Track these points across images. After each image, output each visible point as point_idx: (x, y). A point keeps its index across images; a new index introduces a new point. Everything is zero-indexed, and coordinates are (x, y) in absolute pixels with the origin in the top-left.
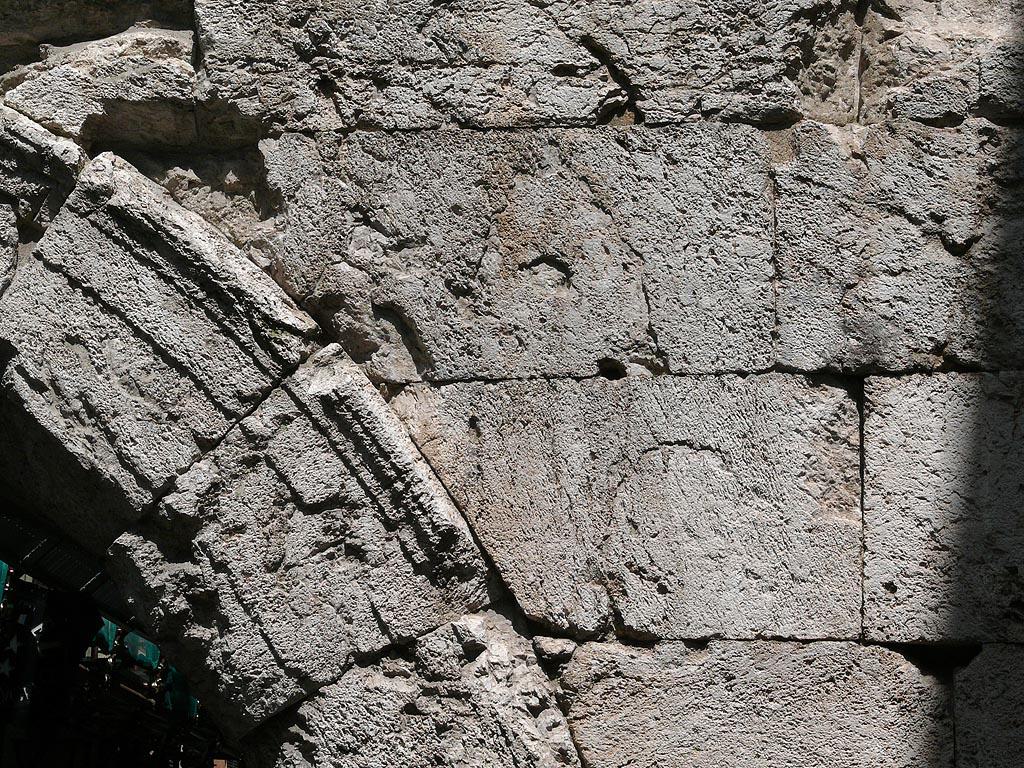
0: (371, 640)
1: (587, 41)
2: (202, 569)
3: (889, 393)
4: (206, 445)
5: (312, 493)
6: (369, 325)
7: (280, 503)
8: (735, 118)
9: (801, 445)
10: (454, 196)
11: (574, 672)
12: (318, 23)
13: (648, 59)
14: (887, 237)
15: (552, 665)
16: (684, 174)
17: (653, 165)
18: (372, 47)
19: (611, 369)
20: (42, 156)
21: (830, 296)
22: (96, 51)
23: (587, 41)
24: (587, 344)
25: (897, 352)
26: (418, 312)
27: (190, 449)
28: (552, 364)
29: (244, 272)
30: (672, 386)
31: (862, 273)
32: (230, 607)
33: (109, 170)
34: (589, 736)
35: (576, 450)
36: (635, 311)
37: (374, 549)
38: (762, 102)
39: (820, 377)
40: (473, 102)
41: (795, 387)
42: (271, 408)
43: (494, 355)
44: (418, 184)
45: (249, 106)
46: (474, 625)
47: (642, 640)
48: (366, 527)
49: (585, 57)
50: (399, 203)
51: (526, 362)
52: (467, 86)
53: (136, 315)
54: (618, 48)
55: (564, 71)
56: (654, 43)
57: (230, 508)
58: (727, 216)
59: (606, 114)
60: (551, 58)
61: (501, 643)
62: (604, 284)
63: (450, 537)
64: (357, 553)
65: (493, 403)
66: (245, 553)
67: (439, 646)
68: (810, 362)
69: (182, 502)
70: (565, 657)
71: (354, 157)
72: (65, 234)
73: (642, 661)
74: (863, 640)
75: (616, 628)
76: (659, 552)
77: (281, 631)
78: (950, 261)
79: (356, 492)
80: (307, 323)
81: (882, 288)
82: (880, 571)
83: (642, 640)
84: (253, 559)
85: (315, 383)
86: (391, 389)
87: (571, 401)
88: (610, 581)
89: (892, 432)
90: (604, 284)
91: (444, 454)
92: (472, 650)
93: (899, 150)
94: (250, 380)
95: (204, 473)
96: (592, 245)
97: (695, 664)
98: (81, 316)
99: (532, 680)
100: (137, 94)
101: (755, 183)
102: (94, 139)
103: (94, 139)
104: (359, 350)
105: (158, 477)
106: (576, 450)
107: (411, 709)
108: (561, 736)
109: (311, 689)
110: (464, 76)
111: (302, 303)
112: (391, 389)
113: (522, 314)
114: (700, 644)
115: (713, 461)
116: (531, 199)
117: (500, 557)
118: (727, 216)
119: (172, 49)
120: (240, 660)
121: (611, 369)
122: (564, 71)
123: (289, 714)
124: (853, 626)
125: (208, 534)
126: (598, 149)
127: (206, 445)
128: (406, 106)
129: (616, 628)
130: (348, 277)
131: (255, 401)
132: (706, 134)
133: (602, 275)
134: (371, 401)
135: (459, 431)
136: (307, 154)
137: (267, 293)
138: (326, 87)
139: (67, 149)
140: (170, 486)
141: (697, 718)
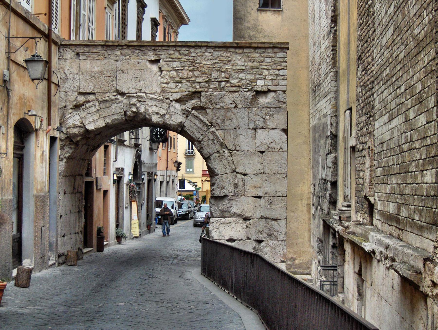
0: (216, 151)
1: (233, 101)
2: (202, 145)
3: (258, 131)
4: (202, 135)
5: (211, 139)
6: (215, 125)
7: (208, 140)
8: (246, 108)
9: (251, 135)
10: (222, 114)
11: (232, 153)
12: (211, 99)
13: (238, 102)
14: (258, 118)
15: (230, 153)
16: (241, 112)
17: (239, 112)
18: (216, 101)
19: (235, 128)
20: (188, 111)
21: (253, 122)
22: (193, 101)
23: (233, 101)
24: (233, 127)
25: (259, 127)
26: (219, 124)
27: (201, 135)
28: (230, 128)
29: (205, 120)
30: (241, 130)
31: (256, 121)
32: (204, 148)
33: (193, 112)
34: (234, 159)
35: (232, 135)
36: (237, 124)
37: (216, 143)
38: (248, 106)
39: (253, 129)
40: (224, 106)
41: (250, 130)
42: (207, 132)
43: (226, 127)
44: (219, 113)
45: (205, 106)
46: (224, 150)
47: (238, 151)
48: (215, 142)
49: (233, 102)
50: (218, 115)
51: (228, 128)
52: (224, 105)
53: (196, 124)
54: (236, 102)
55: (231, 103)
56: (239, 101)
57: (204, 140)
58: (245, 116)
59: (235, 107)
60: (230, 103)
61: (226, 151)
62: (235, 121)
63: (222, 142)
64: (215, 144)
65: (225, 131)
66: (205, 144)
67: (221, 151)
68: (252, 128)
69: (200, 139)
70: (232, 152)
71: (214, 111)
72: (190, 117)
73: (238, 153)
74: (256, 151)
75: (235, 150)
76: (239, 143)
77: (208, 150)
78: (263, 119)
79: (214, 139)
80: (210, 125)
81: (257, 122)
82: (257, 145)
83: (238, 151)
84: (206, 144)
85: (211, 130)
86: (217, 130)
87: (232, 131)
88: (235, 146)
89: (258, 134)
90: (235, 121)
91: (222, 136)
92: (224, 152)
93: (259, 111)
94: (206, 130)
95: (202, 137)
96: (234, 118)
97: (242, 153)
98: (191, 124)
99: (229, 154)
100: (196, 105)
101: (247, 113)
102: (193, 109)
103: (193, 109)
104: (214, 127)
105: (198, 137)
106: (232, 135)
107: (219, 156)
108: (231, 159)
109: (211, 155)
110: (223, 104)
111: (210, 123)
112: (217, 130)
113: (228, 124)
114: (243, 151)
115: (244, 136)
116: (229, 114)
117: (226, 144)
118: (245, 116)
119: (199, 101)
120: (205, 152)
121: (235, 128)
122: (231, 103)
123: (209, 157)
124: (255, 150)
125: (202, 142)
126: (234, 110)
127: (202, 135)
128: (218, 106)
129: (235, 150)
130: (213, 121)
131: (206, 131)
132: (243, 109)
133: (235, 121)
134: (216, 131)
135: (223, 134)
136: (210, 110)
137: (207, 122)
138: (212, 104)
139: (190, 110)
140: (199, 138)
141: (242, 157)
